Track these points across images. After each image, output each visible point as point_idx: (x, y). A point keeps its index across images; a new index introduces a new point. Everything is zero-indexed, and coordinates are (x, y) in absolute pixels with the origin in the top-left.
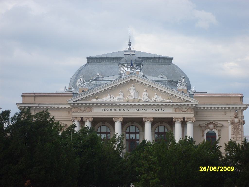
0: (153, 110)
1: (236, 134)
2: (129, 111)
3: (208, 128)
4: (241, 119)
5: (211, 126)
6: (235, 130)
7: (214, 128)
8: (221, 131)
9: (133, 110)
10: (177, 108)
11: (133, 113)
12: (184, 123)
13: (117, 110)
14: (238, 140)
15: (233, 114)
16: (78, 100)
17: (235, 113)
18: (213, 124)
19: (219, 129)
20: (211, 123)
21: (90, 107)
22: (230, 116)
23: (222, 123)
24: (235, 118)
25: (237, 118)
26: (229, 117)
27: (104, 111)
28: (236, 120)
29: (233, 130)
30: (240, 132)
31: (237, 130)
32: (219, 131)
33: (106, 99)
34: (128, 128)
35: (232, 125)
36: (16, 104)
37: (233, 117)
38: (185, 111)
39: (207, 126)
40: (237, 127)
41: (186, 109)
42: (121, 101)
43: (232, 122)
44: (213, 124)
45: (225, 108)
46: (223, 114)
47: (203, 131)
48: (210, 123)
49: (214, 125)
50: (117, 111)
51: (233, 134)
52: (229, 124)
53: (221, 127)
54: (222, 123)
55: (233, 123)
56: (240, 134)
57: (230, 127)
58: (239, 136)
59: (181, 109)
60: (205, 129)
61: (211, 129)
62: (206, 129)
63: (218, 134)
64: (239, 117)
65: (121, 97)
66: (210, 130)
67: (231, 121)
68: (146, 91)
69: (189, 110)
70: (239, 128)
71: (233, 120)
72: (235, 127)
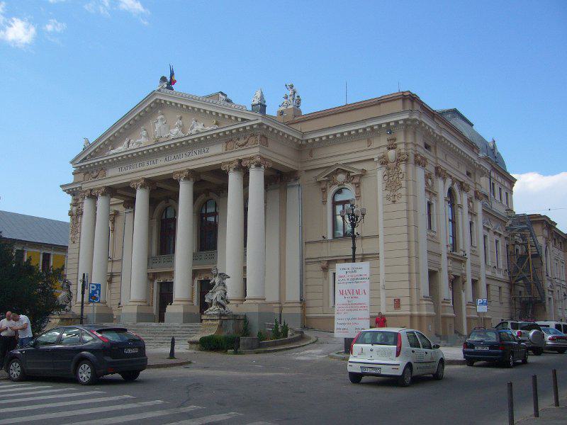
3: (335, 184)
4: (403, 151)
7: (347, 182)
8: (361, 187)
9: (161, 161)
10: (228, 139)
11: (159, 168)
13: (146, 164)
15: (383, 141)
16: (85, 159)
17: (389, 137)
18: (344, 171)
21: (102, 168)
22: (379, 148)
23: (360, 167)
24: (389, 149)
25: (392, 148)
27: (122, 173)
30: (403, 183)
33: (121, 148)
34: (204, 207)
36: (62, 186)
37: (385, 149)
38: (243, 145)
39: (330, 179)
42: (142, 145)
43: (383, 160)
45: (364, 129)
46: (363, 145)
47: (324, 191)
48: (338, 171)
52: (379, 166)
53: (361, 176)
54: (360, 167)
55: (384, 162)
57: (380, 173)
58: (399, 191)
61: (342, 185)
64: (398, 146)
65: (143, 140)
67: (379, 158)
68: (181, 119)
69: (253, 139)
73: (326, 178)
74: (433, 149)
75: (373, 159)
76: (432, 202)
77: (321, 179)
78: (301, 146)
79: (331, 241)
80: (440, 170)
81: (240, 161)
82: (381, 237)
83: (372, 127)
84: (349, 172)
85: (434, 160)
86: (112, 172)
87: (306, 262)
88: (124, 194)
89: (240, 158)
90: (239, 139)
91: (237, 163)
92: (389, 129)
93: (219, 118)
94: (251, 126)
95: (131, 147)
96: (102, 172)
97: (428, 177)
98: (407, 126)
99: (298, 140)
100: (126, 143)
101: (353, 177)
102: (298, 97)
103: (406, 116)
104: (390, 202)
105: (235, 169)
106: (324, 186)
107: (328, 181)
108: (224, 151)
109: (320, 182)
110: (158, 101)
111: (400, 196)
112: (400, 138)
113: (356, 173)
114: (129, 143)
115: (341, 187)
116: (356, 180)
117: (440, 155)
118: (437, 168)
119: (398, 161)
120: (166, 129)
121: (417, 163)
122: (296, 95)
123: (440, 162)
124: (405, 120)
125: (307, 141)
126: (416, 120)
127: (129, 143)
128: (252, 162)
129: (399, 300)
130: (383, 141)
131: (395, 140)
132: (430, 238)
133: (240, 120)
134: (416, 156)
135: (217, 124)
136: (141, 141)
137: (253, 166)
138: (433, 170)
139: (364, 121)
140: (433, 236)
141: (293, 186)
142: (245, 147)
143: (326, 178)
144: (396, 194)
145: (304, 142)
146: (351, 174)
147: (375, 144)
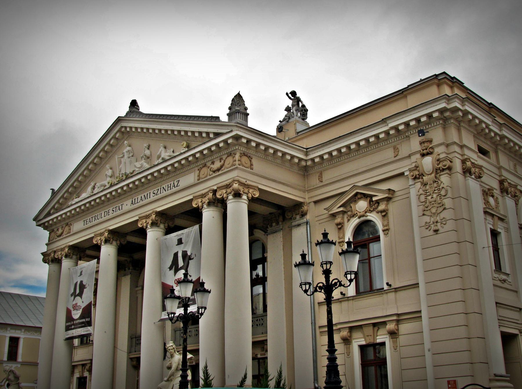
0: (159, 192)
1: (434, 210)
2: (121, 211)
3: (353, 216)
5: (362, 205)
6: (429, 198)
7: (371, 211)
12: (220, 204)
14: (441, 230)
15: (415, 143)
18: (365, 196)
19: (382, 207)
20: (359, 196)
21: (68, 221)
22: (409, 156)
24: (423, 155)
25: (428, 154)
26: (407, 162)
27: (86, 226)
28: (428, 161)
29: (423, 198)
30: (447, 202)
31: (435, 196)
32: (384, 214)
35: (419, 185)
37: (418, 156)
38: (218, 170)
40: (435, 185)
41: (220, 162)
42: (105, 188)
44: (365, 196)
45: (387, 133)
49: (369, 199)
50: (104, 219)
51: (424, 215)
52: (411, 182)
53: (388, 199)
56: (445, 209)
58: (442, 215)
59: (212, 166)
60: (346, 220)
61: (363, 216)
62: (349, 220)
63: (384, 226)
64: (437, 150)
66: (359, 218)
67: (410, 170)
70: (442, 185)
71: (417, 167)
72: (428, 187)
73: (341, 209)
74: (492, 155)
75: (402, 174)
76: (499, 230)
77: (335, 210)
78: (306, 169)
79: (353, 298)
80: (506, 184)
81: (215, 192)
82: (422, 285)
83: (396, 128)
84: (371, 196)
85: (496, 170)
86: (78, 226)
87: (321, 332)
88: (87, 251)
89: (215, 188)
90: (213, 163)
91: (211, 195)
92: (421, 128)
93: (190, 139)
94: (225, 141)
95: (95, 191)
96: (67, 228)
97: (487, 193)
98: (445, 120)
99: (300, 160)
100: (89, 189)
101: (378, 202)
102: (303, 106)
103: (442, 105)
104: (431, 232)
105: (209, 204)
106: (338, 220)
107: (344, 212)
108: (197, 182)
109: (334, 216)
110: (123, 129)
111: (444, 222)
112: (437, 135)
113: (381, 196)
114: (94, 188)
115: (362, 219)
116: (382, 207)
117: (504, 161)
118: (501, 182)
119: (438, 171)
120: (129, 162)
121: (467, 172)
122: (300, 105)
123: (505, 174)
124: (442, 111)
125: (313, 160)
126: (456, 109)
127: (94, 188)
128: (229, 191)
129: (455, 381)
130: (415, 143)
131: (430, 141)
132: (499, 283)
133: (211, 136)
134: (464, 162)
135: (188, 146)
136: (102, 183)
137: (230, 197)
138: (495, 185)
139: (384, 121)
140: (504, 281)
141: (299, 225)
142: (220, 172)
143: (341, 209)
144: (438, 219)
145: (309, 163)
146: (374, 199)
147: (404, 151)
